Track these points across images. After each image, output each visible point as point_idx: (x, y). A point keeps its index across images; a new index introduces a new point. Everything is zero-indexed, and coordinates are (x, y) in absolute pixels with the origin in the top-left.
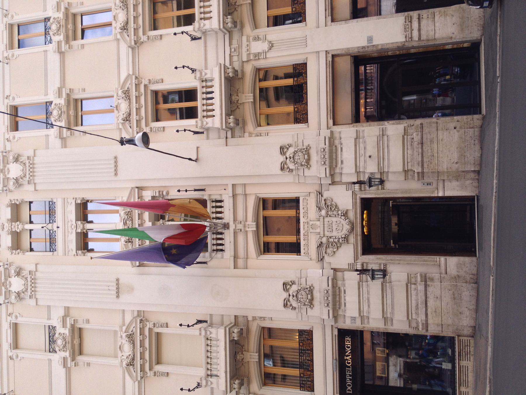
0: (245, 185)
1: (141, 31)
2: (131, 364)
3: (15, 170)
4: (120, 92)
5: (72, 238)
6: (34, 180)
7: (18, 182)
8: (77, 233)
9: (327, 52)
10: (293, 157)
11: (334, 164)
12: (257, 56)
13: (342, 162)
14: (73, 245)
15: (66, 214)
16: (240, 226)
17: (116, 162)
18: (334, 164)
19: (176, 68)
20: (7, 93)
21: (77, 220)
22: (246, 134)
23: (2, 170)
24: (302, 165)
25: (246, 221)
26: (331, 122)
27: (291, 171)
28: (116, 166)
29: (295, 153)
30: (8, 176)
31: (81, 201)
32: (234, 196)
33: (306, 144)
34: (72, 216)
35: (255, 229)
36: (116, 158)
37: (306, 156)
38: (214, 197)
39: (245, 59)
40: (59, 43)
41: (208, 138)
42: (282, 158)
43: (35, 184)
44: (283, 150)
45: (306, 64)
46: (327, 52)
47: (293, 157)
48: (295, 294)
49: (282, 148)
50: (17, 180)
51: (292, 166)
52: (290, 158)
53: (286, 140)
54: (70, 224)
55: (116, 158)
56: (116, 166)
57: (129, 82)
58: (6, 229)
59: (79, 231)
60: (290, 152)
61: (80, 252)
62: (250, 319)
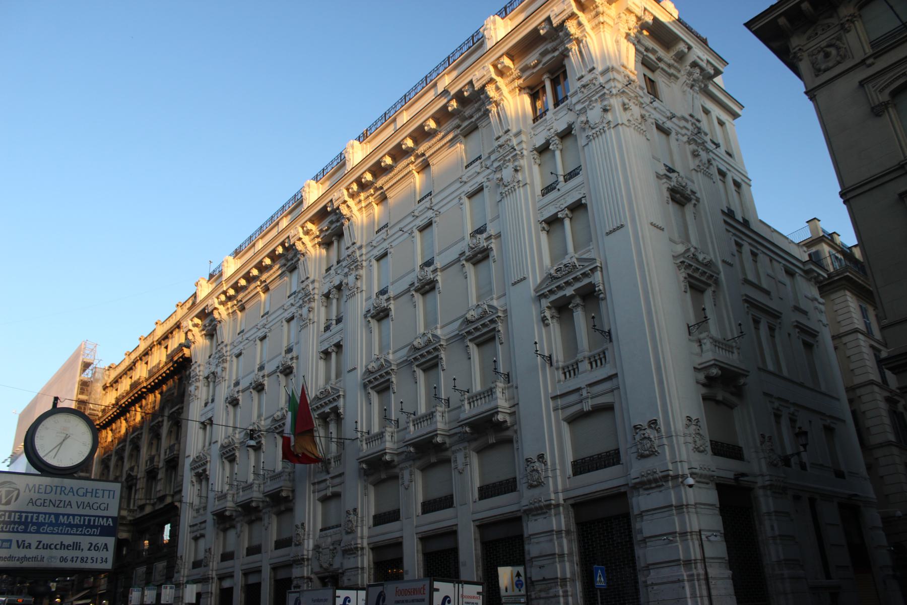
2: (468, 322)
3: (594, 115)
11: (648, 486)
14: (547, 214)
15: (569, 193)
17: (618, 228)
18: (648, 486)
25: (592, 398)
28: (614, 230)
34: (570, 200)
37: (647, 452)
44: (653, 423)
54: (563, 202)
55: (622, 226)
56: (614, 230)
60: (650, 433)
61: (544, 225)
62: (515, 427)
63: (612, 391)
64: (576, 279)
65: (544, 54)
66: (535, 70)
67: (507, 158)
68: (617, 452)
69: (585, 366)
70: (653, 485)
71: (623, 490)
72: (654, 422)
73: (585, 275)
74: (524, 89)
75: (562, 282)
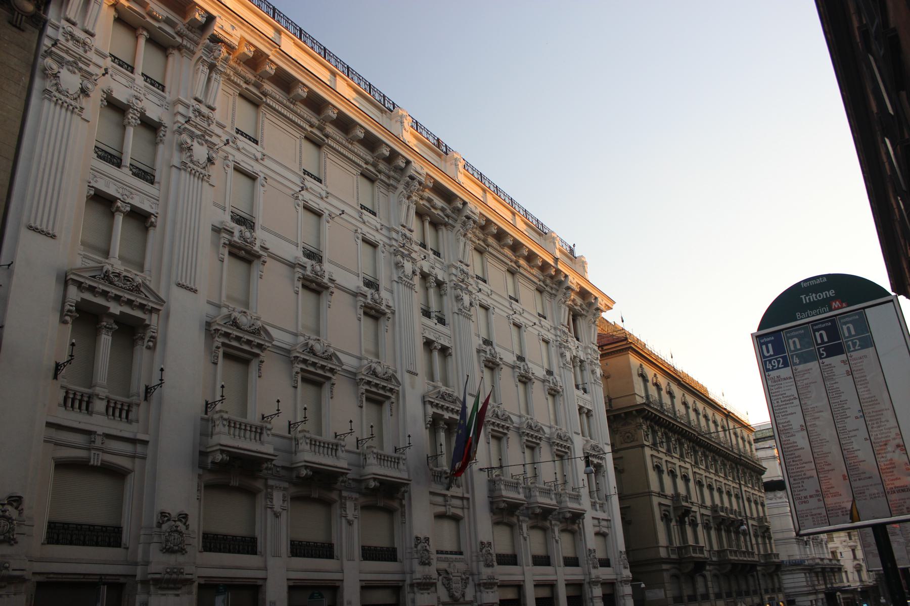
0: (144, 458)
1: (304, 367)
3: (200, 152)
4: (259, 323)
5: (112, 190)
6: (185, 170)
7: (184, 148)
8: (115, 199)
9: (265, 579)
10: (176, 531)
12: (269, 497)
13: (164, 595)
15: (141, 196)
16: (98, 443)
17: (191, 290)
19: (278, 401)
20: (269, 180)
21: (132, 206)
22: (201, 472)
23: (203, 136)
24: (167, 541)
26: (202, 581)
27: (159, 525)
29: (180, 533)
30: (195, 140)
31: (152, 223)
32: (133, 441)
33: (188, 548)
35: (92, 463)
36: (195, 291)
37: (176, 548)
38: (134, 409)
39: (271, 482)
40: (304, 268)
41: (202, 419)
42: (174, 514)
43: (180, 169)
44: (183, 517)
45: (256, 554)
46: (265, 579)
47: (176, 531)
48: (7, 514)
49: (186, 516)
50: (190, 149)
51: (165, 527)
52: (177, 527)
53: (193, 522)
55: (195, 291)
57: (267, 339)
58: (134, 101)
59: (119, 204)
61: (92, 193)
63: (133, 457)
64: (130, 303)
65: (167, 21)
66: (149, 19)
67: (80, 65)
68: (118, 530)
69: (99, 406)
70: (172, 586)
71: (122, 580)
72: (186, 516)
73: (142, 307)
74: (116, 10)
75: (114, 291)
